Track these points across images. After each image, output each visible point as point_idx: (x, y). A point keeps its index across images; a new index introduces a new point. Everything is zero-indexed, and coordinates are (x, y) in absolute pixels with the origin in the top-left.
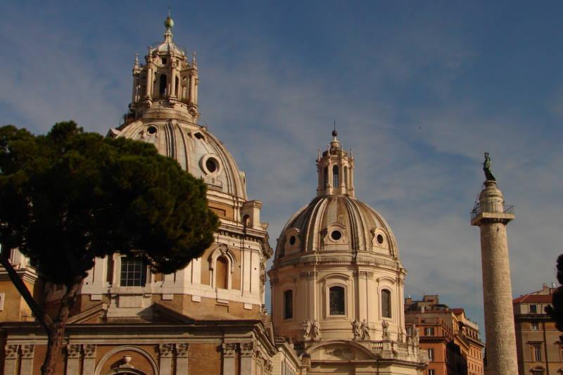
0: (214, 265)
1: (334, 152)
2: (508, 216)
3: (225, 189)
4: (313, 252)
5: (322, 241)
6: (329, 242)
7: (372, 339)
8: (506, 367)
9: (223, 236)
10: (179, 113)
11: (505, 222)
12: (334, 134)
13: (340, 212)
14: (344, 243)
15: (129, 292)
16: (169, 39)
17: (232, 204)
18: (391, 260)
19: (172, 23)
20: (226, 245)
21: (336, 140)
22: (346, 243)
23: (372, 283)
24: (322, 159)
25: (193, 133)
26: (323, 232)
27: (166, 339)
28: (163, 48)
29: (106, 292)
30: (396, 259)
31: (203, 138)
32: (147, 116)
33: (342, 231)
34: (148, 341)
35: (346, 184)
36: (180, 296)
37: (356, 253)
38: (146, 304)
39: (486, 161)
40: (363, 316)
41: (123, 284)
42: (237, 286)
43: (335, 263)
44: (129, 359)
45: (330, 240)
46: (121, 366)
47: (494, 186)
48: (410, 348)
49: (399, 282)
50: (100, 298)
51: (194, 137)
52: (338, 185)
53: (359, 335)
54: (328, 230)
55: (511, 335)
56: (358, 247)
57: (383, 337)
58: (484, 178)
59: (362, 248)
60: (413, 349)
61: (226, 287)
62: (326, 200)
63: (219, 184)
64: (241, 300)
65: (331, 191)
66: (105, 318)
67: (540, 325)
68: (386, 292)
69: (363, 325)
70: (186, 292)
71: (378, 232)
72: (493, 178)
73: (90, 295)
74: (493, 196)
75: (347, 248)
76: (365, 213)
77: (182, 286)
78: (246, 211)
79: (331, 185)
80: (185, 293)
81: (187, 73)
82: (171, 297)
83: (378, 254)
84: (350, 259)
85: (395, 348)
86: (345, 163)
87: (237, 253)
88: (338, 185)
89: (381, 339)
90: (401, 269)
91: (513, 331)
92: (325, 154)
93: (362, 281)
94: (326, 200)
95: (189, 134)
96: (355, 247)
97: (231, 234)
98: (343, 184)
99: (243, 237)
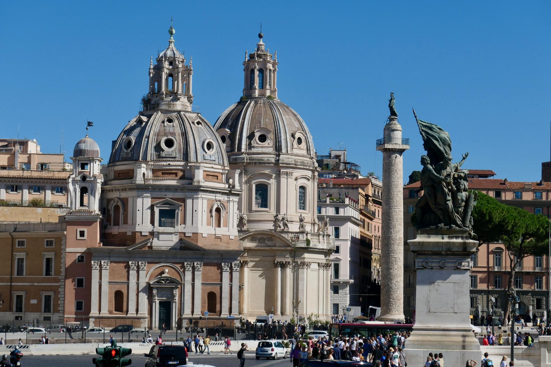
0: (214, 213)
1: (259, 56)
2: (405, 147)
4: (242, 153)
5: (250, 144)
6: (256, 145)
7: (290, 230)
8: (394, 263)
9: (218, 195)
11: (401, 152)
12: (260, 36)
14: (268, 146)
15: (165, 231)
16: (172, 45)
17: (221, 171)
18: (308, 159)
19: (174, 31)
20: (220, 201)
21: (261, 43)
22: (271, 145)
23: (291, 181)
24: (248, 60)
25: (196, 122)
26: (251, 137)
28: (169, 53)
29: (151, 231)
30: (312, 158)
31: (201, 124)
32: (163, 107)
35: (270, 85)
36: (195, 234)
37: (279, 155)
38: (175, 239)
39: (391, 99)
40: (283, 211)
41: (160, 225)
43: (261, 163)
44: (167, 270)
45: (257, 143)
46: (163, 275)
47: (395, 122)
48: (321, 237)
49: (314, 179)
50: (147, 234)
51: (196, 124)
52: (262, 86)
53: (280, 227)
54: (256, 134)
55: (400, 238)
56: (281, 149)
57: (299, 228)
58: (389, 113)
59: (284, 151)
60: (323, 237)
61: (219, 226)
62: (253, 102)
64: (228, 234)
65: (257, 93)
66: (151, 247)
68: (303, 188)
69: (283, 219)
71: (297, 135)
72: (395, 115)
73: (141, 232)
74: (394, 130)
75: (271, 150)
77: (197, 228)
78: (229, 176)
79: (257, 87)
80: (199, 232)
81: (187, 71)
82: (191, 235)
83: (297, 155)
84: (273, 161)
85: (309, 237)
86: (270, 66)
87: (225, 204)
88: (262, 86)
89: (298, 230)
90: (316, 168)
91: (402, 236)
92: (252, 57)
93: (283, 180)
94: (253, 102)
95: (193, 123)
96: (278, 149)
97: (223, 194)
98: (268, 87)
99: (230, 193)
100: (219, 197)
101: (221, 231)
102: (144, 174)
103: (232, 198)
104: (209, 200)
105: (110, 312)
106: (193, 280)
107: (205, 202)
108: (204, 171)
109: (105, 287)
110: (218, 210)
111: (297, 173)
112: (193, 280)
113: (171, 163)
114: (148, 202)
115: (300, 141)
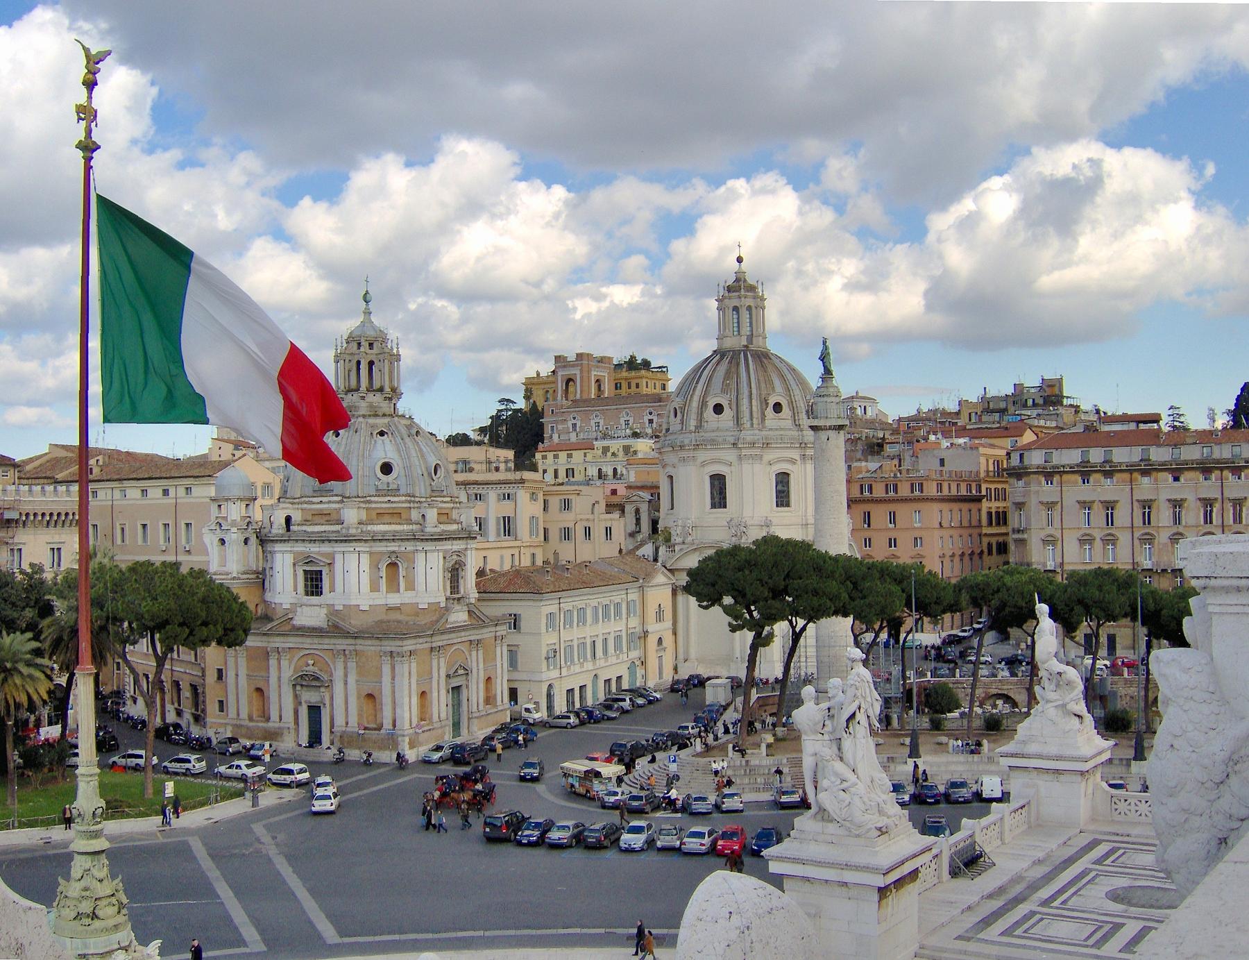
0: (383, 573)
3: (401, 492)
10: (371, 406)
13: (728, 375)
27: (341, 644)
33: (725, 404)
34: (326, 647)
42: (411, 586)
50: (288, 606)
63: (395, 487)
67: (1056, 478)
70: (354, 602)
75: (731, 424)
76: (760, 373)
78: (423, 511)
82: (341, 608)
100: (393, 547)
101: (401, 598)
102: (288, 520)
103: (420, 545)
104: (371, 553)
105: (251, 719)
106: (346, 676)
107: (365, 559)
108: (367, 509)
109: (243, 681)
110: (393, 565)
111: (770, 455)
112: (346, 676)
113: (324, 499)
114: (289, 559)
115: (778, 407)
